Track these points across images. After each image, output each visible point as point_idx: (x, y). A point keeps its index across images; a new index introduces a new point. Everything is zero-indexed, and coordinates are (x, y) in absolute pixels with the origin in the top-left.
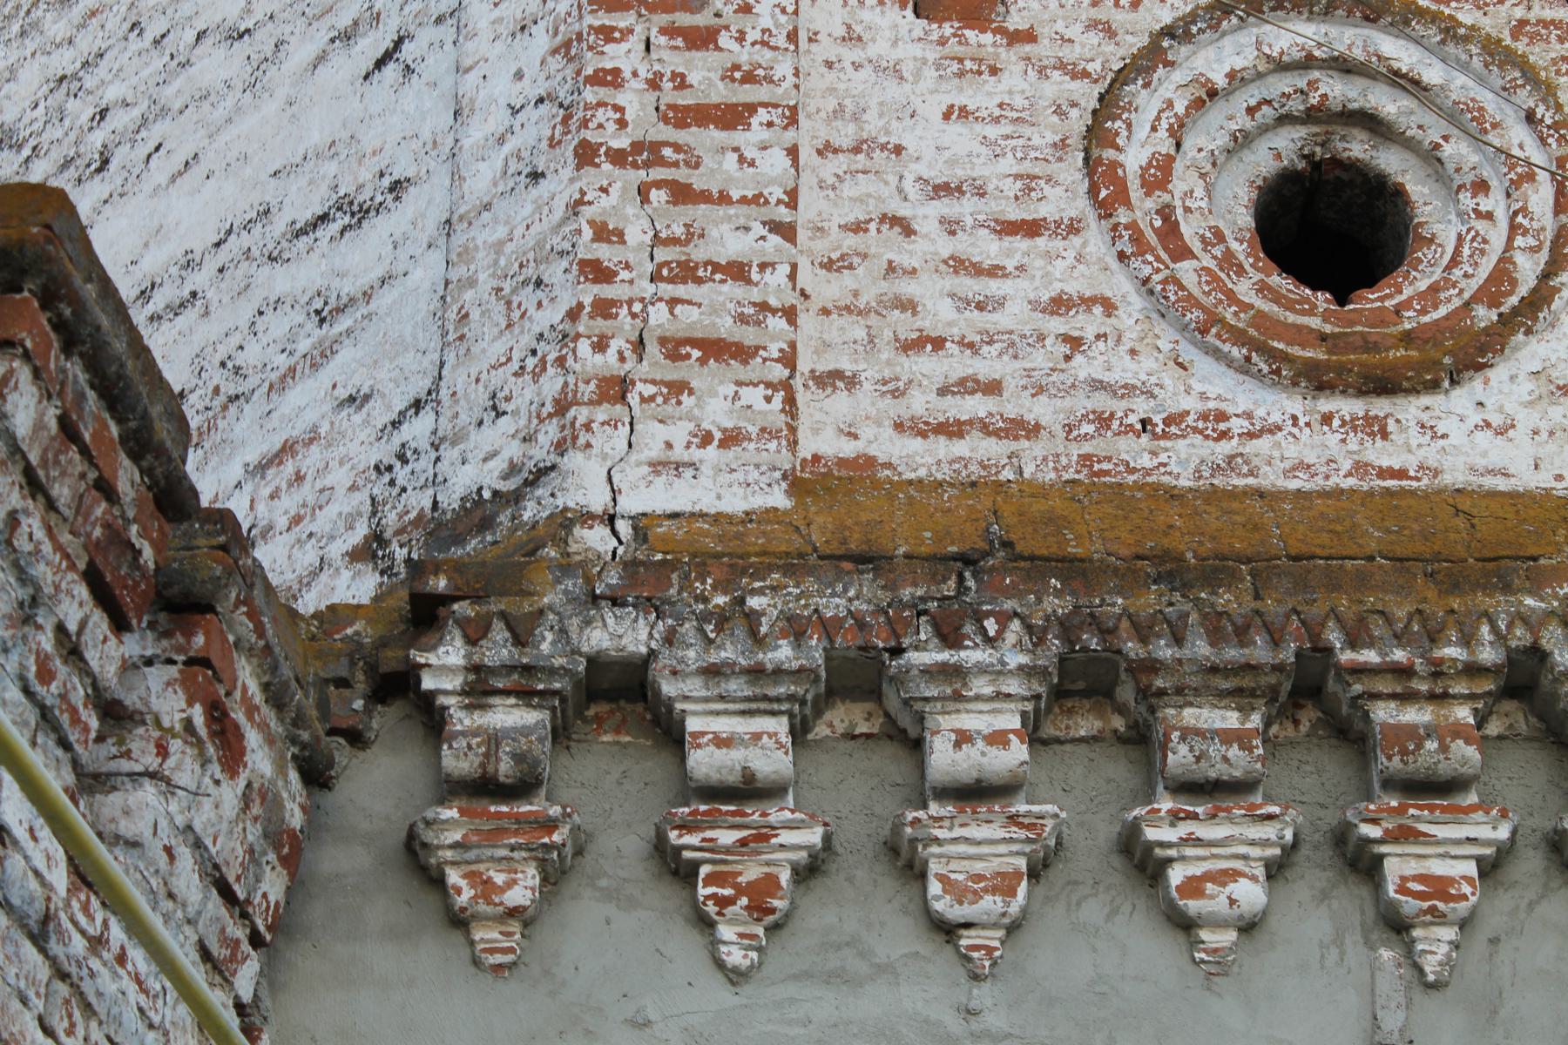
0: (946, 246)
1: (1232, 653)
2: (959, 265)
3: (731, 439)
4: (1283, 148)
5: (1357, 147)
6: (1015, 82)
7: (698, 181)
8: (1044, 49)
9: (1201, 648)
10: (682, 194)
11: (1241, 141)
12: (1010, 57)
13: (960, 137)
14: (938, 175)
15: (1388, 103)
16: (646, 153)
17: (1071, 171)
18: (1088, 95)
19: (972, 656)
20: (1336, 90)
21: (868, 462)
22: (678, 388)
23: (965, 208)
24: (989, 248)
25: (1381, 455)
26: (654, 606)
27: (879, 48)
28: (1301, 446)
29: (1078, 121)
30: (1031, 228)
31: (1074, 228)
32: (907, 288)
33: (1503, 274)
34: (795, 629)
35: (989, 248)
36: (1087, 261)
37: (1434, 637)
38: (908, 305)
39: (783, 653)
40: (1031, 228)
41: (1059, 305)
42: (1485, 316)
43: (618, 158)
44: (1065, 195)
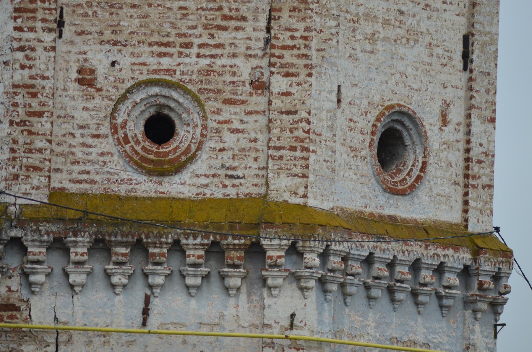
0: (81, 141)
1: (125, 239)
2: (84, 145)
3: (38, 188)
4: (152, 111)
5: (166, 112)
6: (98, 101)
7: (33, 130)
8: (104, 93)
9: (119, 238)
10: (30, 133)
11: (143, 112)
12: (96, 95)
13: (85, 114)
14: (82, 123)
15: (173, 105)
16: (23, 123)
17: (107, 123)
18: (111, 104)
19: (80, 239)
20: (162, 101)
21: (63, 189)
22: (28, 177)
23: (86, 131)
24: (90, 141)
25: (161, 189)
26: (23, 228)
27: (70, 92)
28: (146, 186)
29: (110, 110)
30: (98, 136)
31: (107, 137)
32: (73, 150)
33: (189, 148)
34: (48, 233)
35: (90, 141)
36: (108, 144)
37: (161, 237)
38: (73, 154)
39: (45, 238)
40: (98, 136)
41: (102, 154)
42: (183, 158)
43: (17, 124)
44: (105, 130)
